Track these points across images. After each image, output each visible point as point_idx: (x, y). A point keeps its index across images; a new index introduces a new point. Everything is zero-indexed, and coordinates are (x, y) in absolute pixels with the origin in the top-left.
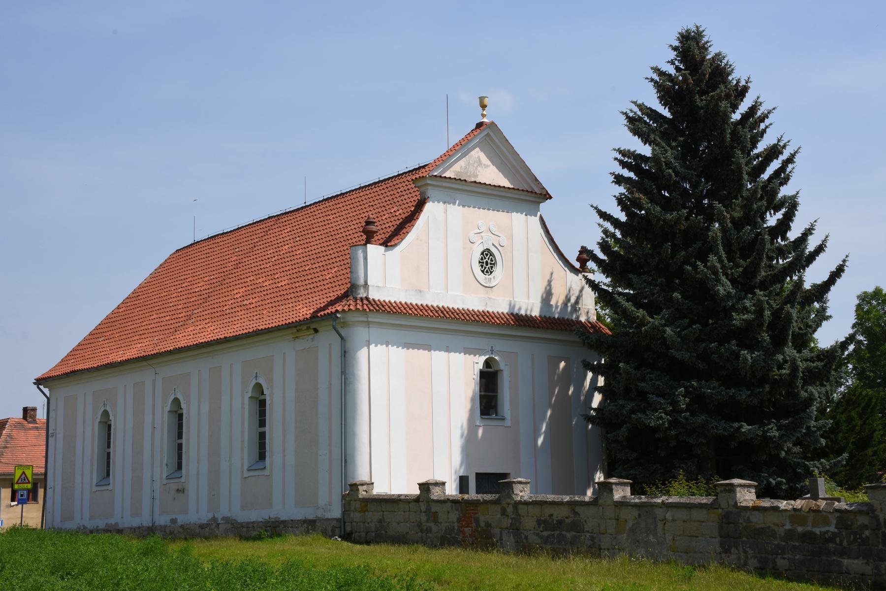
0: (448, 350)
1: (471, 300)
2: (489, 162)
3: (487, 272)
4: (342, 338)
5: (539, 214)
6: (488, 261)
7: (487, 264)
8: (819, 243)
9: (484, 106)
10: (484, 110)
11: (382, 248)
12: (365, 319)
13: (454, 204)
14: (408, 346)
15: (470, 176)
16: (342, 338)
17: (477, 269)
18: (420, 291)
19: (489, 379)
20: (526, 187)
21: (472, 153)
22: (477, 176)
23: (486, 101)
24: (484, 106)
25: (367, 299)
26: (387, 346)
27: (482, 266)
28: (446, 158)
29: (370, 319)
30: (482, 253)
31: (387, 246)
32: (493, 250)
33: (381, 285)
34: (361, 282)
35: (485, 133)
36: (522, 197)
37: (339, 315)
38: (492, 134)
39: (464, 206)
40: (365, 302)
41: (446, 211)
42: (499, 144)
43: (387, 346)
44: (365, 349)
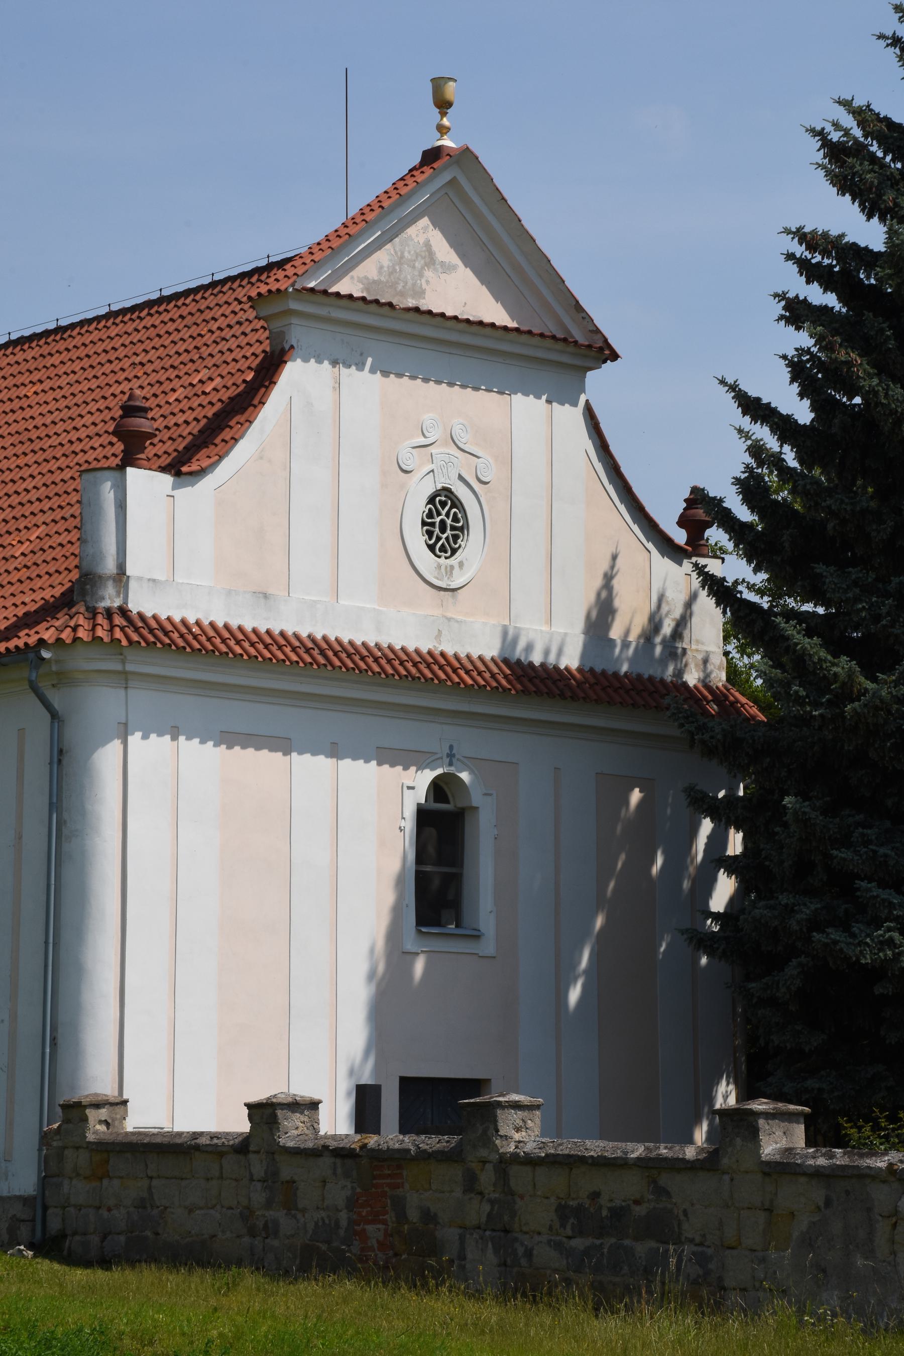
0: (335, 752)
1: (403, 625)
3: (443, 549)
4: (54, 715)
5: (583, 399)
6: (445, 521)
9: (443, 105)
10: (443, 114)
11: (167, 479)
12: (119, 667)
14: (229, 738)
15: (402, 294)
16: (54, 715)
17: (417, 540)
18: (266, 596)
19: (441, 829)
20: (552, 328)
21: (411, 231)
22: (421, 293)
23: (451, 90)
24: (443, 105)
25: (124, 611)
26: (174, 738)
27: (430, 534)
29: (130, 667)
30: (431, 500)
31: (178, 474)
32: (461, 491)
33: (160, 576)
34: (110, 566)
35: (446, 177)
36: (540, 354)
37: (46, 654)
40: (118, 620)
44: (117, 744)
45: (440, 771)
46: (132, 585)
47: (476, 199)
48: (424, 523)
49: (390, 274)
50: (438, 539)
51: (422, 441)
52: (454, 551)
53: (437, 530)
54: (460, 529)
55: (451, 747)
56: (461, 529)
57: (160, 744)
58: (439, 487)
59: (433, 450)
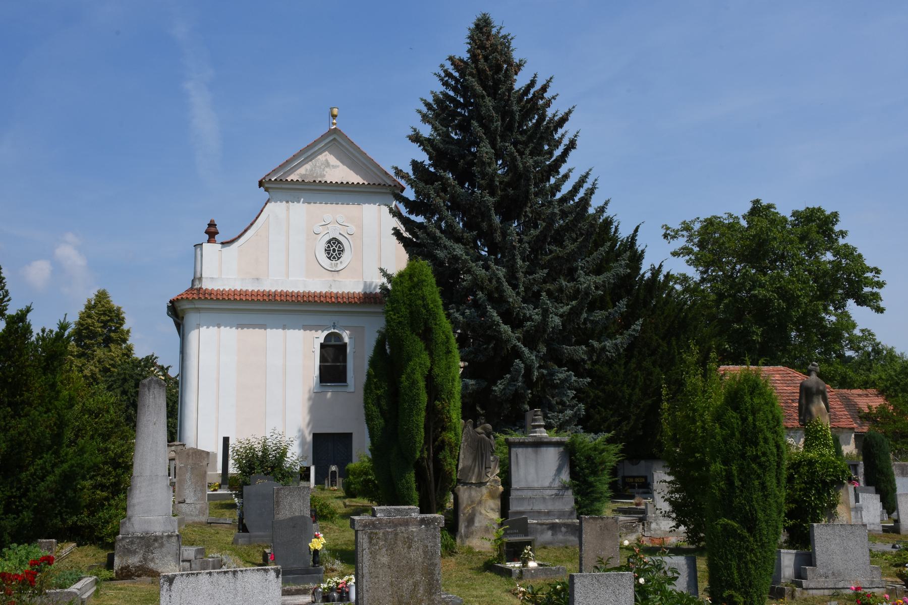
1: (317, 284)
2: (338, 163)
3: (334, 258)
6: (334, 249)
8: (601, 204)
9: (334, 116)
13: (299, 202)
17: (323, 257)
20: (380, 181)
21: (320, 157)
22: (324, 176)
23: (335, 111)
25: (201, 288)
26: (219, 327)
27: (328, 254)
28: (288, 164)
30: (329, 242)
32: (341, 238)
34: (198, 275)
35: (331, 138)
38: (338, 139)
39: (309, 203)
42: (347, 146)
43: (219, 327)
44: (197, 331)
46: (204, 280)
47: (344, 144)
52: (339, 258)
54: (341, 251)
57: (213, 330)
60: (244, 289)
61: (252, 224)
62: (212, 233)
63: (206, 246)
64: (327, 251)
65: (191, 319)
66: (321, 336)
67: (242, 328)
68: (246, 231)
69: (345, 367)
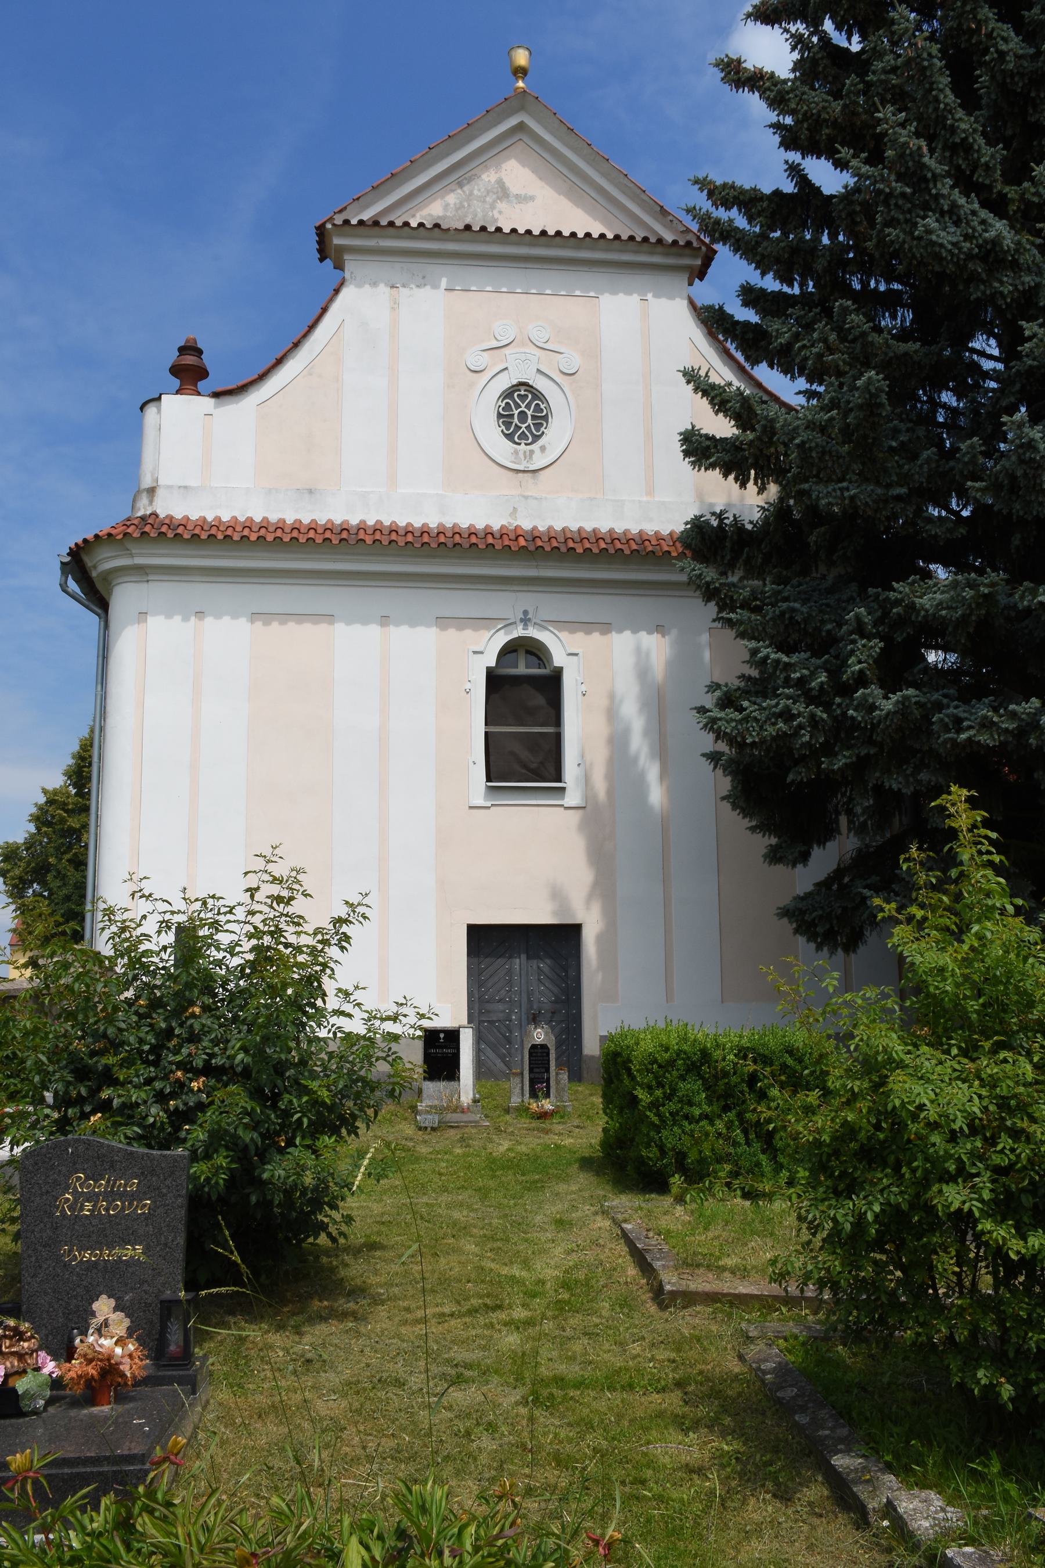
3: (523, 436)
6: (523, 412)
7: (523, 416)
11: (211, 401)
18: (310, 491)
23: (521, 58)
25: (155, 514)
27: (508, 425)
29: (139, 561)
30: (508, 394)
32: (541, 384)
35: (513, 121)
41: (395, 306)
45: (515, 635)
46: (160, 493)
48: (500, 416)
49: (457, 209)
50: (518, 428)
51: (496, 344)
52: (536, 438)
53: (516, 420)
54: (542, 419)
55: (526, 613)
56: (545, 418)
58: (515, 382)
59: (507, 351)
60: (273, 518)
61: (296, 345)
62: (189, 373)
63: (171, 402)
64: (504, 418)
65: (125, 597)
66: (487, 647)
67: (267, 623)
68: (279, 362)
69: (557, 740)
